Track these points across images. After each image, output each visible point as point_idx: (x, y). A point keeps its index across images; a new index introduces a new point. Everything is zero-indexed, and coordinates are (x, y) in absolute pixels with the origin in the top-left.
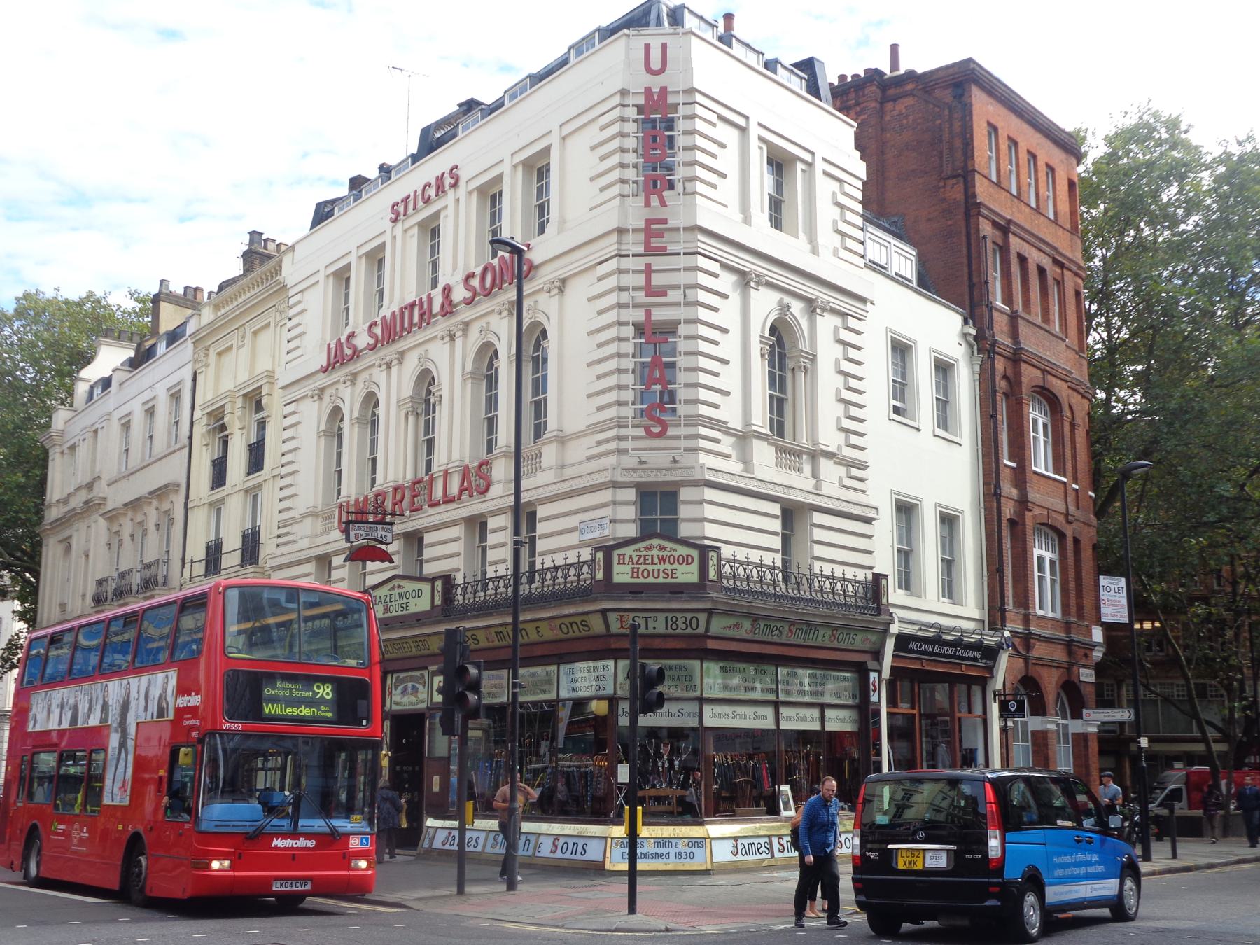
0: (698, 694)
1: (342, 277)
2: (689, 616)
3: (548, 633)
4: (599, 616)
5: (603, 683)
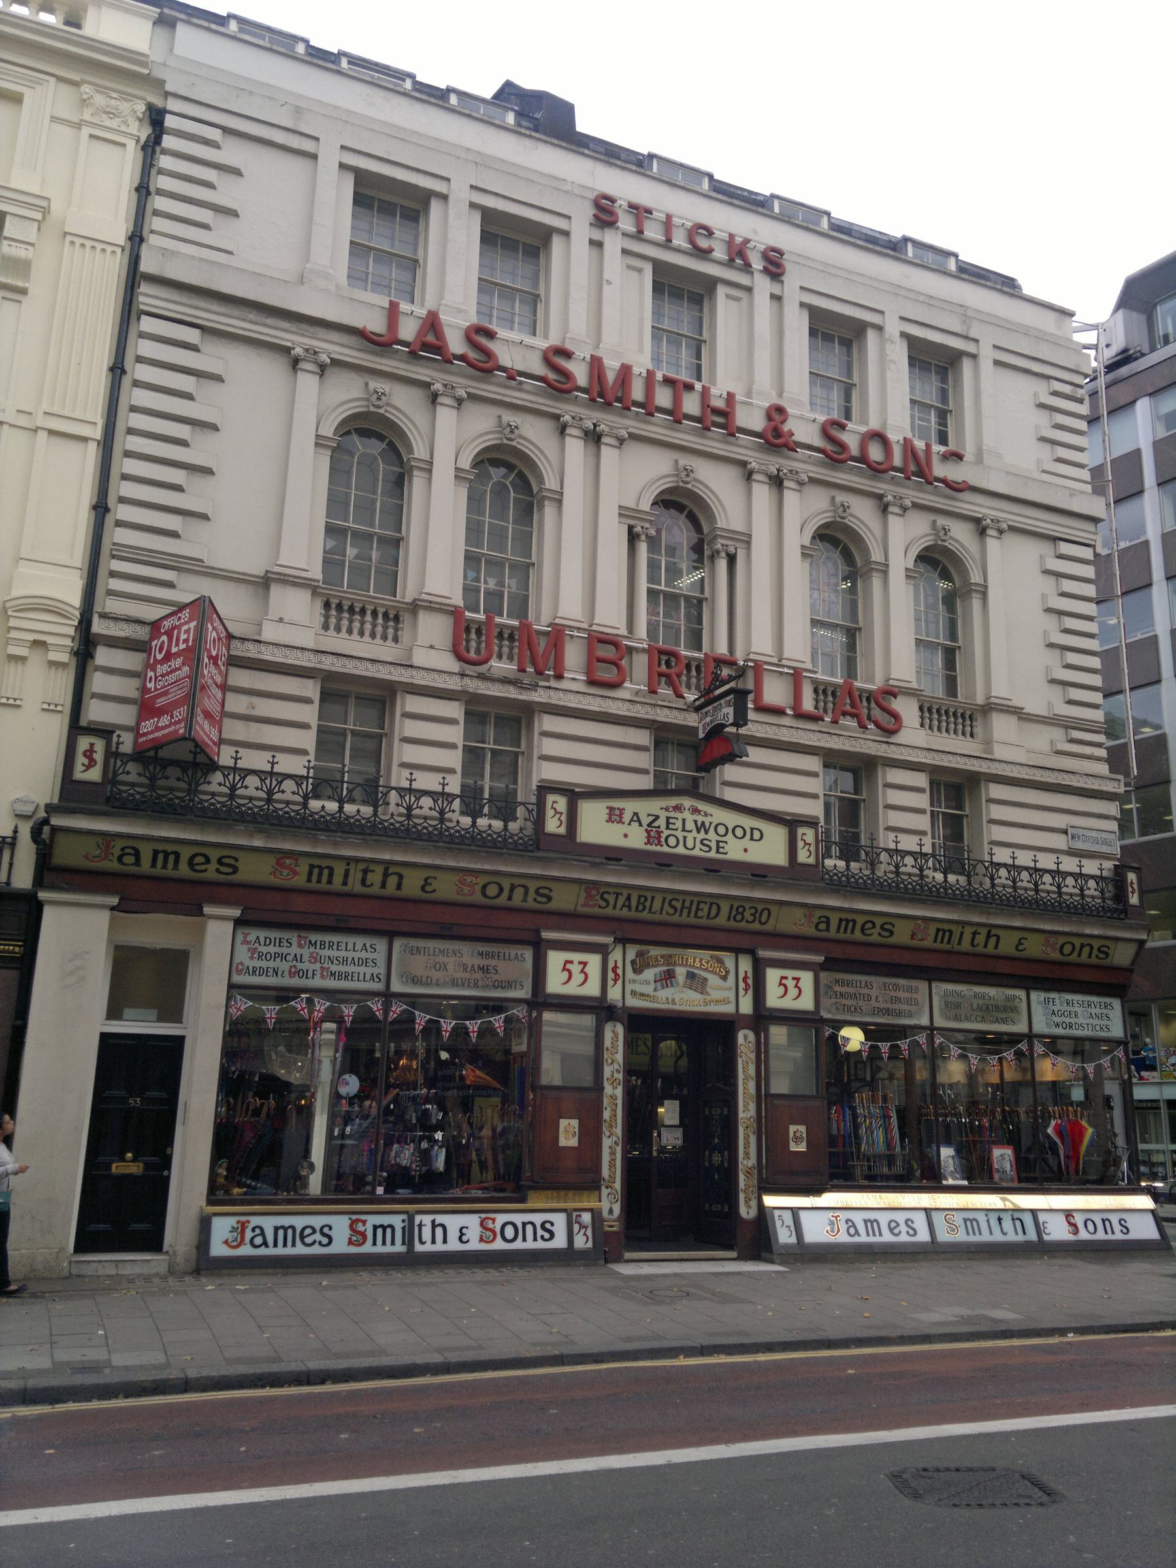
3: (1035, 948)
5: (1105, 1022)
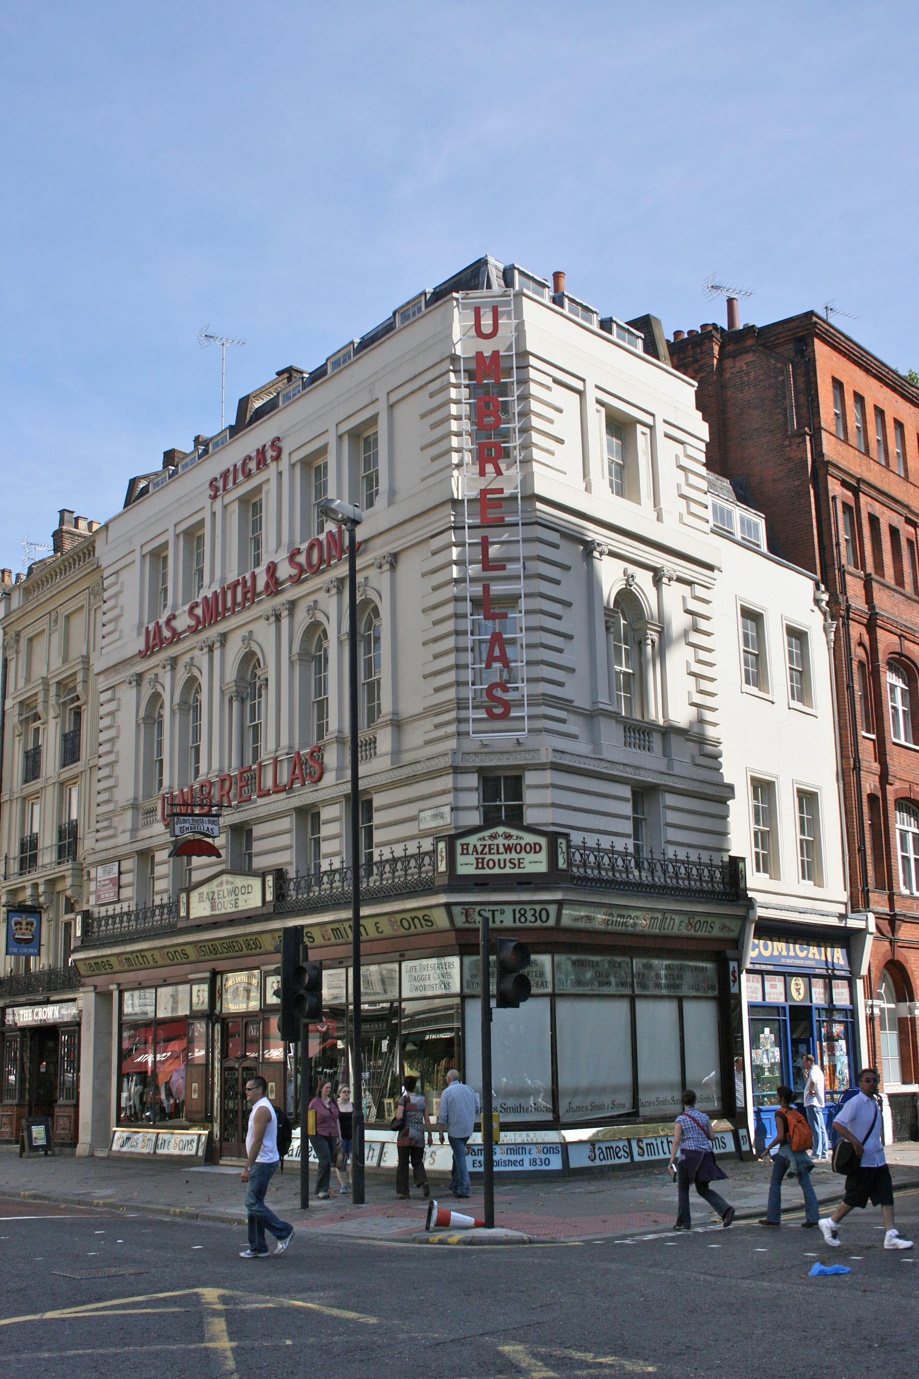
0: (549, 990)
1: (158, 556)
2: (538, 908)
4: (443, 909)
